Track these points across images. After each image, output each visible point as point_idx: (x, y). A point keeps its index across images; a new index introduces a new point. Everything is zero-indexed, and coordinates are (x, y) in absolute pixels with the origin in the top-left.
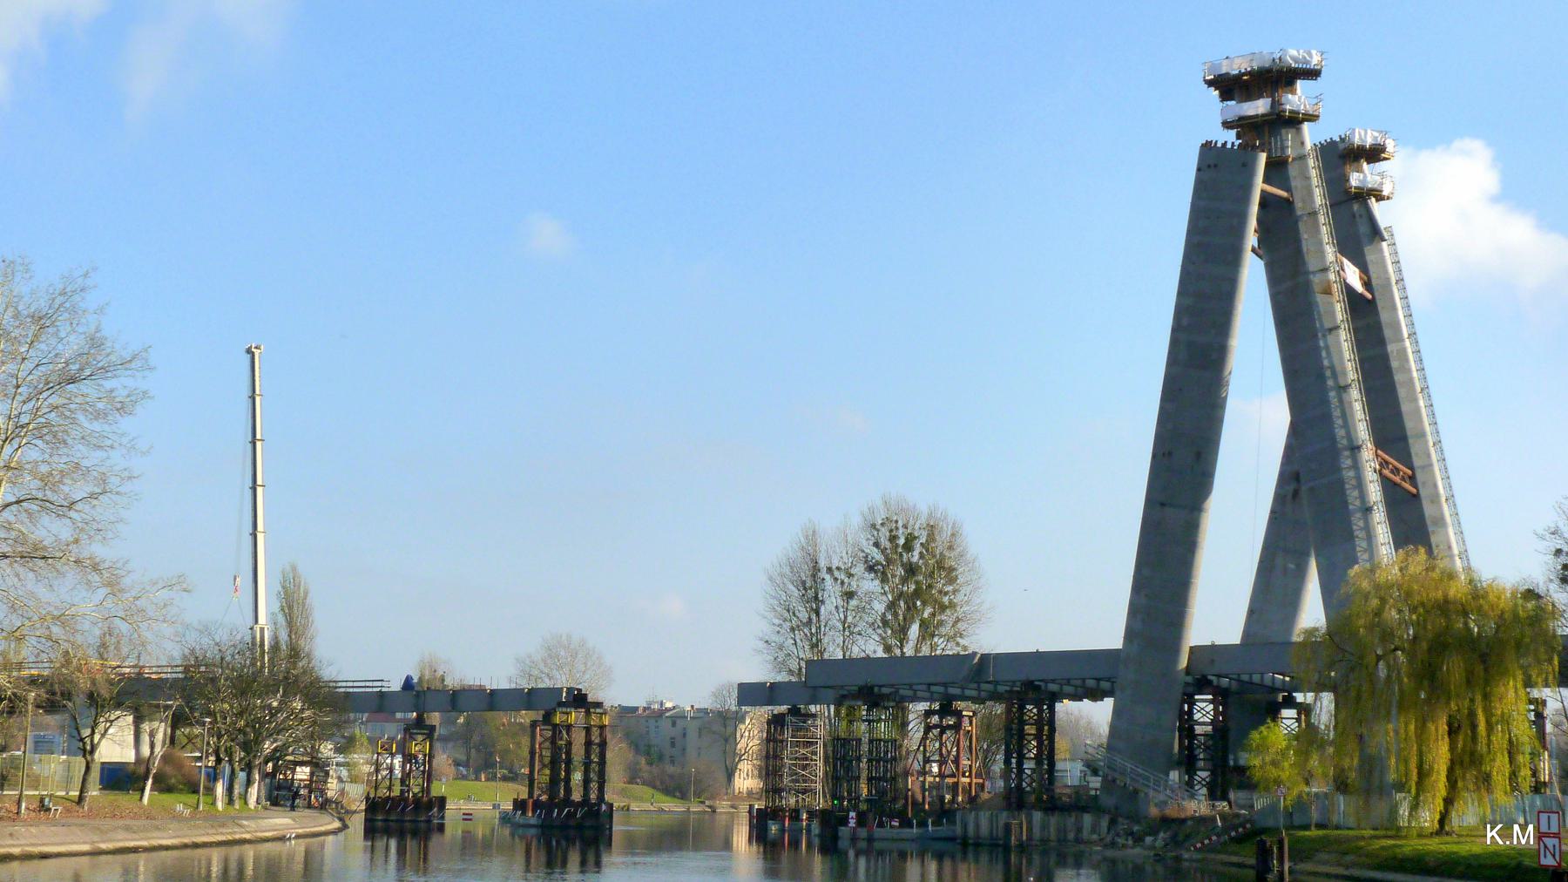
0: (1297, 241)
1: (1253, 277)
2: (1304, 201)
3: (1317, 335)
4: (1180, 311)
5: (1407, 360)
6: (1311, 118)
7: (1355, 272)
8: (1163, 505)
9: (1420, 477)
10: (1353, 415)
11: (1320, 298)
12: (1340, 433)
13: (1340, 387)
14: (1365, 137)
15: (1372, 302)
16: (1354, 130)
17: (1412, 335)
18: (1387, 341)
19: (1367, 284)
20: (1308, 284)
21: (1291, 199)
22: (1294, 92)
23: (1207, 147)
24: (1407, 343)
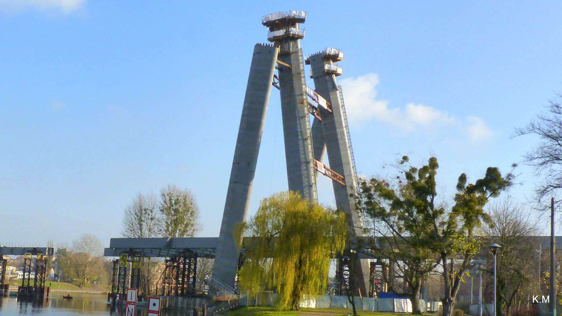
3: (296, 119)
5: (344, 135)
6: (301, 37)
7: (324, 101)
9: (347, 179)
10: (308, 151)
11: (299, 105)
12: (302, 157)
13: (304, 139)
15: (332, 113)
18: (337, 128)
19: (330, 106)
21: (291, 68)
22: (295, 27)
23: (258, 46)
24: (345, 129)
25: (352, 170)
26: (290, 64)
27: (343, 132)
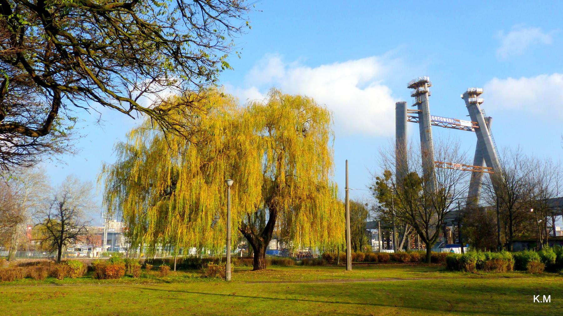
24: (489, 137)
27: (488, 139)
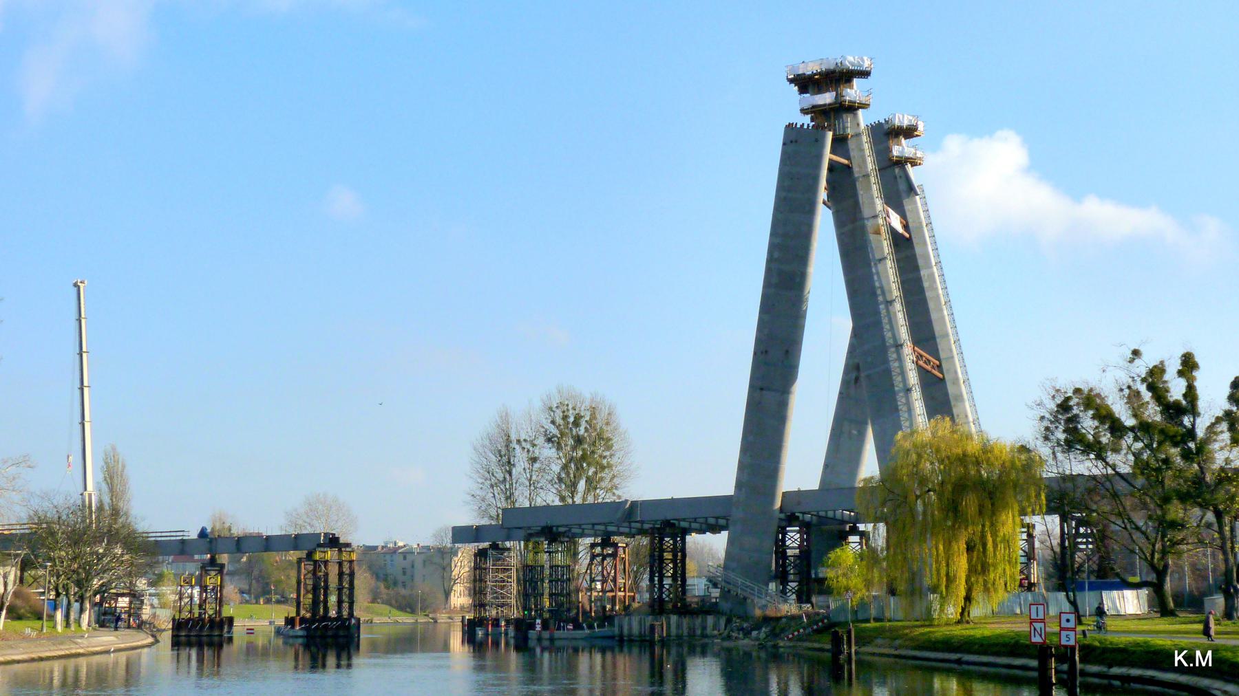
0: (855, 195)
1: (824, 222)
2: (860, 167)
4: (773, 247)
5: (935, 281)
6: (864, 106)
7: (896, 218)
8: (762, 389)
9: (944, 365)
10: (897, 323)
11: (872, 237)
12: (888, 335)
13: (887, 302)
14: (903, 119)
15: (909, 240)
16: (895, 115)
17: (937, 263)
18: (921, 268)
19: (906, 227)
20: (863, 228)
22: (851, 87)
23: (790, 127)
24: (935, 269)
25: (953, 347)
26: (848, 158)
27: (932, 275)
